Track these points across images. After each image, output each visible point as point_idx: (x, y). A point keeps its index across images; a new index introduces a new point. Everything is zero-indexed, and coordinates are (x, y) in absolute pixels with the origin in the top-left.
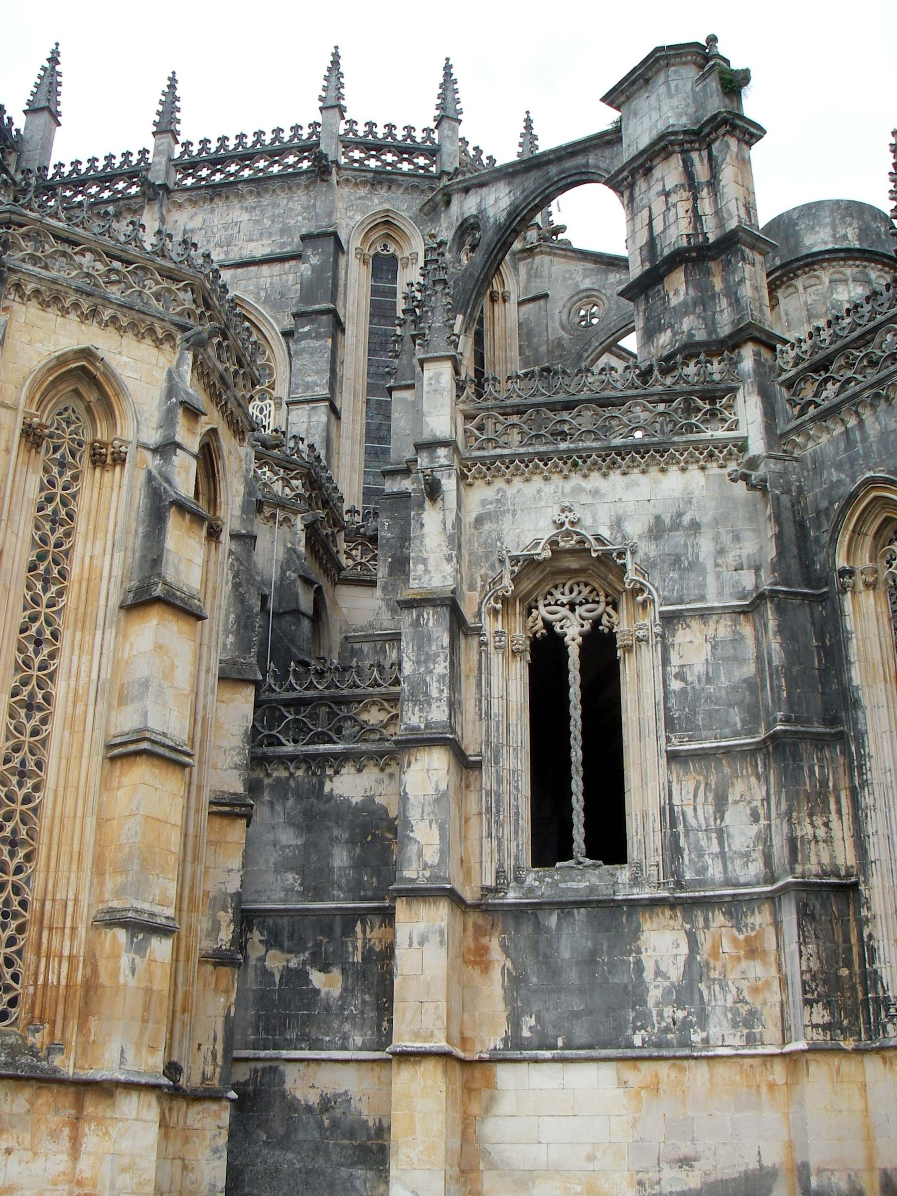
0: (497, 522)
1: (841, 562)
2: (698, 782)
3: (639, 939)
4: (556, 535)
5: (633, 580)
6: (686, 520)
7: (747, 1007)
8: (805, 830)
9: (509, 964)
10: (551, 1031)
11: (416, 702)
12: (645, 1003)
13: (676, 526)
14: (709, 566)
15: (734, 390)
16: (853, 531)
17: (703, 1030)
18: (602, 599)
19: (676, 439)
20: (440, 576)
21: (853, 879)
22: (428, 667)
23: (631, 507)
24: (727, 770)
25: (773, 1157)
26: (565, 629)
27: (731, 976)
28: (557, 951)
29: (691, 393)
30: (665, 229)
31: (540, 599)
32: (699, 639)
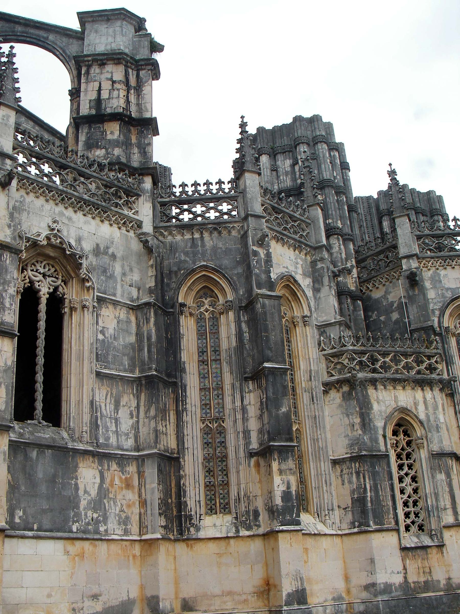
0: (20, 214)
1: (181, 300)
2: (108, 391)
3: (77, 471)
4: (50, 234)
5: (85, 274)
6: (110, 251)
7: (125, 515)
8: (160, 428)
10: (31, 520)
12: (78, 508)
14: (119, 279)
15: (138, 196)
16: (189, 287)
17: (105, 525)
18: (60, 277)
19: (112, 208)
20: (3, 234)
21: (175, 455)
22: (4, 288)
23: (86, 235)
24: (121, 388)
25: (134, 593)
27: (119, 497)
28: (36, 472)
29: (120, 188)
30: (109, 99)
31: (29, 265)
32: (112, 316)
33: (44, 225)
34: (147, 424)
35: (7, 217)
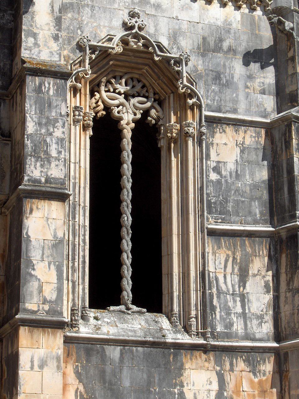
0: (79, 13)
3: (182, 375)
4: (127, 35)
5: (185, 86)
6: (225, 45)
9: (81, 388)
11: (38, 158)
13: (218, 49)
14: (241, 86)
18: (151, 95)
20: (48, 51)
22: (48, 130)
23: (185, 26)
24: (249, 250)
26: (121, 115)
28: (120, 379)
32: (231, 143)
33: (117, 23)
34: (290, 300)
35: (52, 24)
